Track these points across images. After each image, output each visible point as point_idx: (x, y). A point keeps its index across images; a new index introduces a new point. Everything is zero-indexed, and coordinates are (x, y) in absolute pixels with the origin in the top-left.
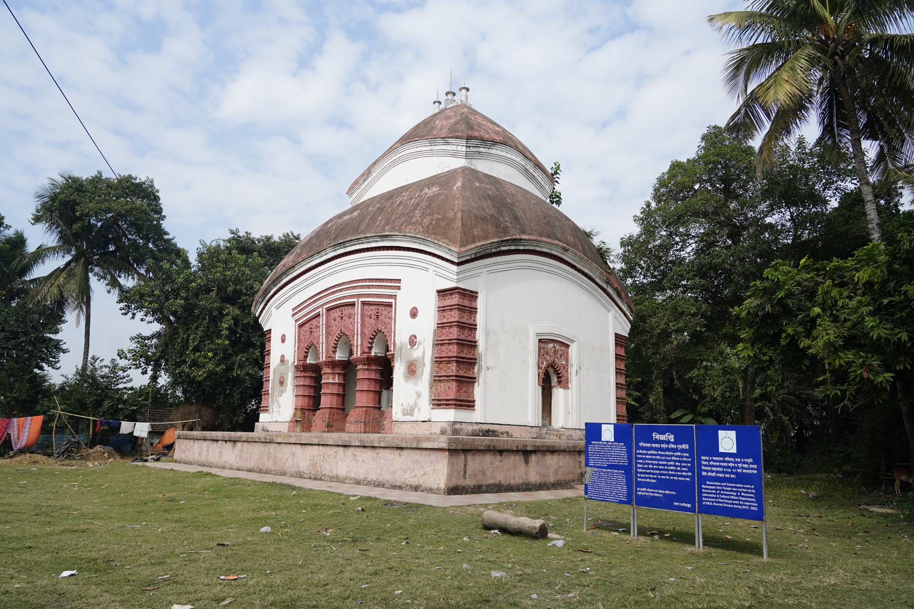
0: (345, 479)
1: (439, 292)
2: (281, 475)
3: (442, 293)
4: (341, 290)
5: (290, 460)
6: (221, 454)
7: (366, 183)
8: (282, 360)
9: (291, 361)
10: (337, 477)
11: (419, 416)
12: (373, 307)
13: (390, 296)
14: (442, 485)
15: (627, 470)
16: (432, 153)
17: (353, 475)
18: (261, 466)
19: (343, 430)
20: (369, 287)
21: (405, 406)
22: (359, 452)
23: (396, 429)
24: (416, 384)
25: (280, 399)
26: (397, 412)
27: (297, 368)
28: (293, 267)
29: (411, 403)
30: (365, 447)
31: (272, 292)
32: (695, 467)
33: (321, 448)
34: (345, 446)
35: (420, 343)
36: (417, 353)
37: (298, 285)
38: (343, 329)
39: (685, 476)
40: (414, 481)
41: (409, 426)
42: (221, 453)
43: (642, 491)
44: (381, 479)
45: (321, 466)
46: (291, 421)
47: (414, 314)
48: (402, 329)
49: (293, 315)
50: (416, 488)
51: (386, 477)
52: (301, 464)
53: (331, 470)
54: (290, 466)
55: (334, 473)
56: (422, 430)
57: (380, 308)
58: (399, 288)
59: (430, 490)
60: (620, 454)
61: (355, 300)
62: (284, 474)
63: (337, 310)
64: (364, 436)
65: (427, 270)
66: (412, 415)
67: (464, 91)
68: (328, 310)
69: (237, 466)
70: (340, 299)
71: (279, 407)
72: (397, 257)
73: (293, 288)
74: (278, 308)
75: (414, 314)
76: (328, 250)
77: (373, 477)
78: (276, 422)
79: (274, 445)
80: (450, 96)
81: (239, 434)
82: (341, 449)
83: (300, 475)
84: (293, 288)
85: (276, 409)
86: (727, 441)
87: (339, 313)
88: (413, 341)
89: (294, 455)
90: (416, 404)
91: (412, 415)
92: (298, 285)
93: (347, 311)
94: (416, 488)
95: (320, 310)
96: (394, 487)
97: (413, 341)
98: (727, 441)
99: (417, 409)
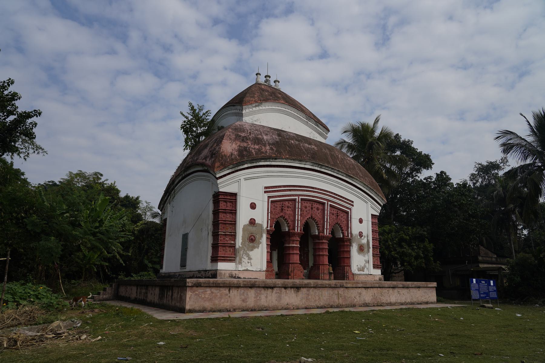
0: (395, 303)
1: (372, 215)
2: (351, 307)
3: (373, 216)
4: (314, 192)
5: (357, 297)
6: (279, 298)
7: (257, 108)
8: (252, 222)
9: (265, 226)
10: (391, 303)
11: (366, 272)
12: (335, 210)
13: (348, 208)
14: (435, 300)
15: (479, 290)
16: (306, 124)
17: (399, 301)
18: (331, 303)
19: (288, 279)
20: (334, 198)
21: (359, 266)
22: (400, 290)
23: (356, 278)
24: (364, 256)
25: (251, 253)
26: (354, 269)
27: (268, 231)
28: (276, 159)
29: (363, 265)
30: (403, 287)
31: (246, 166)
32: (488, 289)
33: (379, 289)
34: (393, 288)
35: (365, 237)
36: (364, 241)
37: (273, 172)
38: (313, 215)
39: (487, 291)
40: (425, 300)
41: (363, 277)
42: (279, 298)
43: (482, 295)
44: (412, 301)
45: (380, 299)
46: (266, 271)
47: (361, 221)
48: (355, 228)
49: (265, 192)
50: (427, 303)
51: (415, 300)
52: (367, 299)
53: (387, 300)
54: (358, 300)
55: (389, 301)
56: (369, 279)
57: (339, 211)
58: (353, 206)
59: (432, 303)
60: (477, 286)
61: (326, 202)
62: (354, 306)
63: (309, 202)
64: (404, 283)
65: (366, 202)
66: (364, 271)
67: (277, 83)
68: (302, 199)
69: (303, 306)
70: (313, 197)
71: (250, 259)
72: (352, 189)
73: (268, 172)
74: (246, 179)
75: (361, 221)
76: (308, 163)
77: (409, 300)
78: (247, 270)
79: (342, 289)
80: (268, 78)
81: (408, 283)
82: (391, 290)
83: (366, 305)
84: (268, 172)
85: (245, 260)
86: (492, 282)
87: (310, 205)
88: (361, 234)
89: (360, 294)
90: (365, 266)
91: (364, 271)
92: (273, 172)
93: (316, 205)
94: (427, 303)
95: (297, 197)
96: (418, 304)
97: (361, 234)
98: (492, 282)
99: (366, 269)
